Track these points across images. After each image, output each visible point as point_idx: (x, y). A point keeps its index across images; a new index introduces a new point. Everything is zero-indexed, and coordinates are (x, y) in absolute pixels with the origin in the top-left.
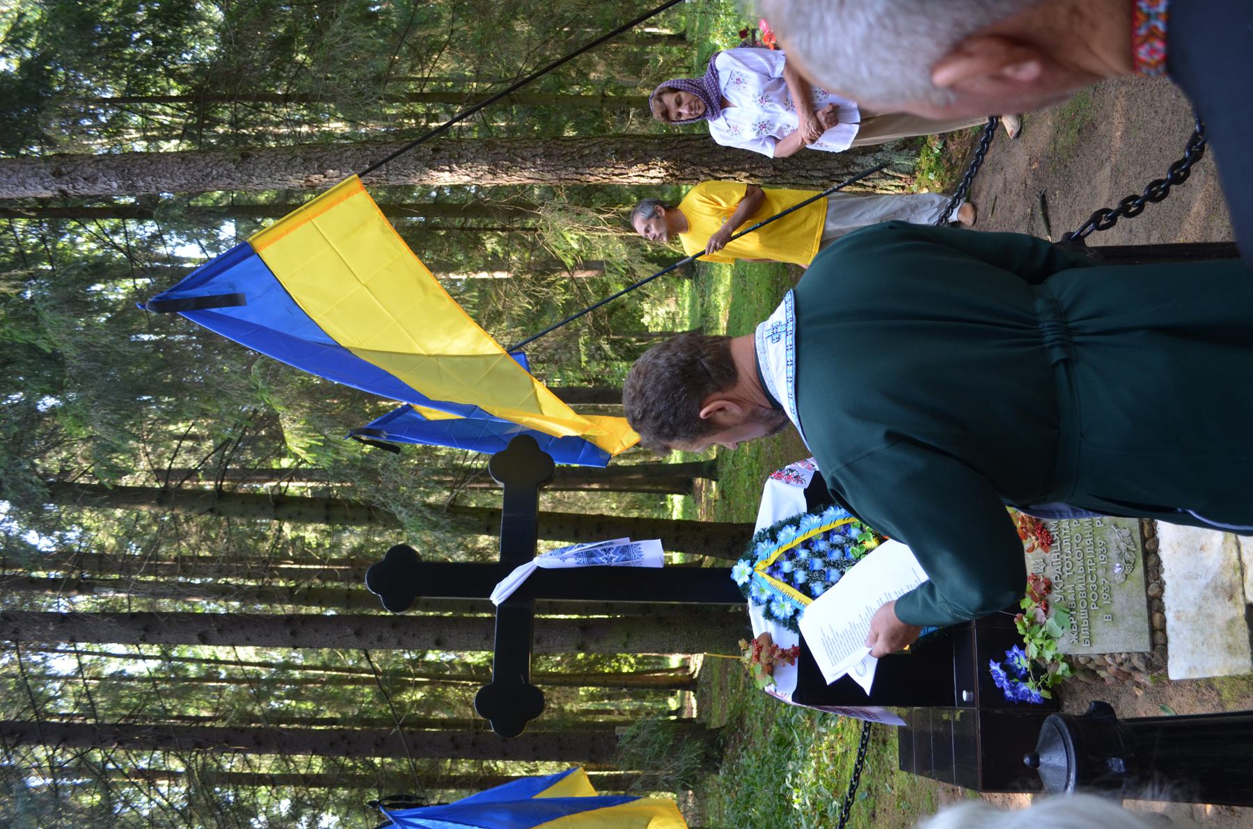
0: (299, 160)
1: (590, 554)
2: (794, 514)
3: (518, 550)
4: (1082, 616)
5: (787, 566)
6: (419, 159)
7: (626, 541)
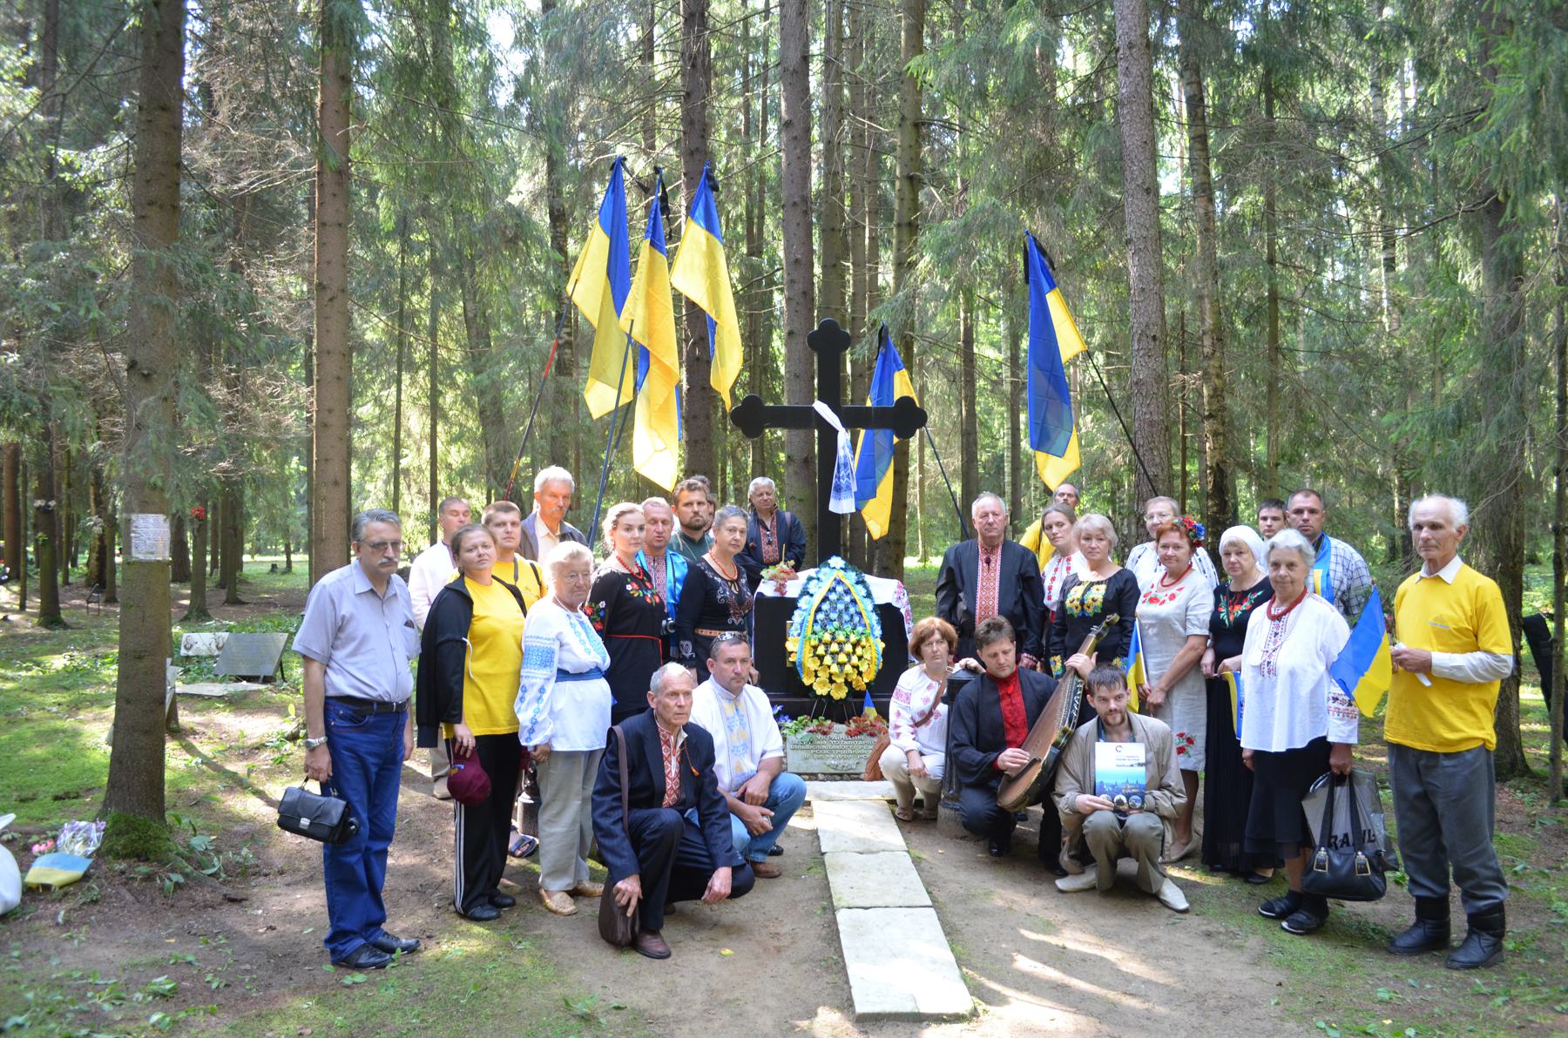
0: (1145, 233)
1: (846, 465)
2: (874, 595)
3: (853, 419)
4: (808, 746)
5: (840, 589)
6: (1147, 326)
7: (854, 488)
